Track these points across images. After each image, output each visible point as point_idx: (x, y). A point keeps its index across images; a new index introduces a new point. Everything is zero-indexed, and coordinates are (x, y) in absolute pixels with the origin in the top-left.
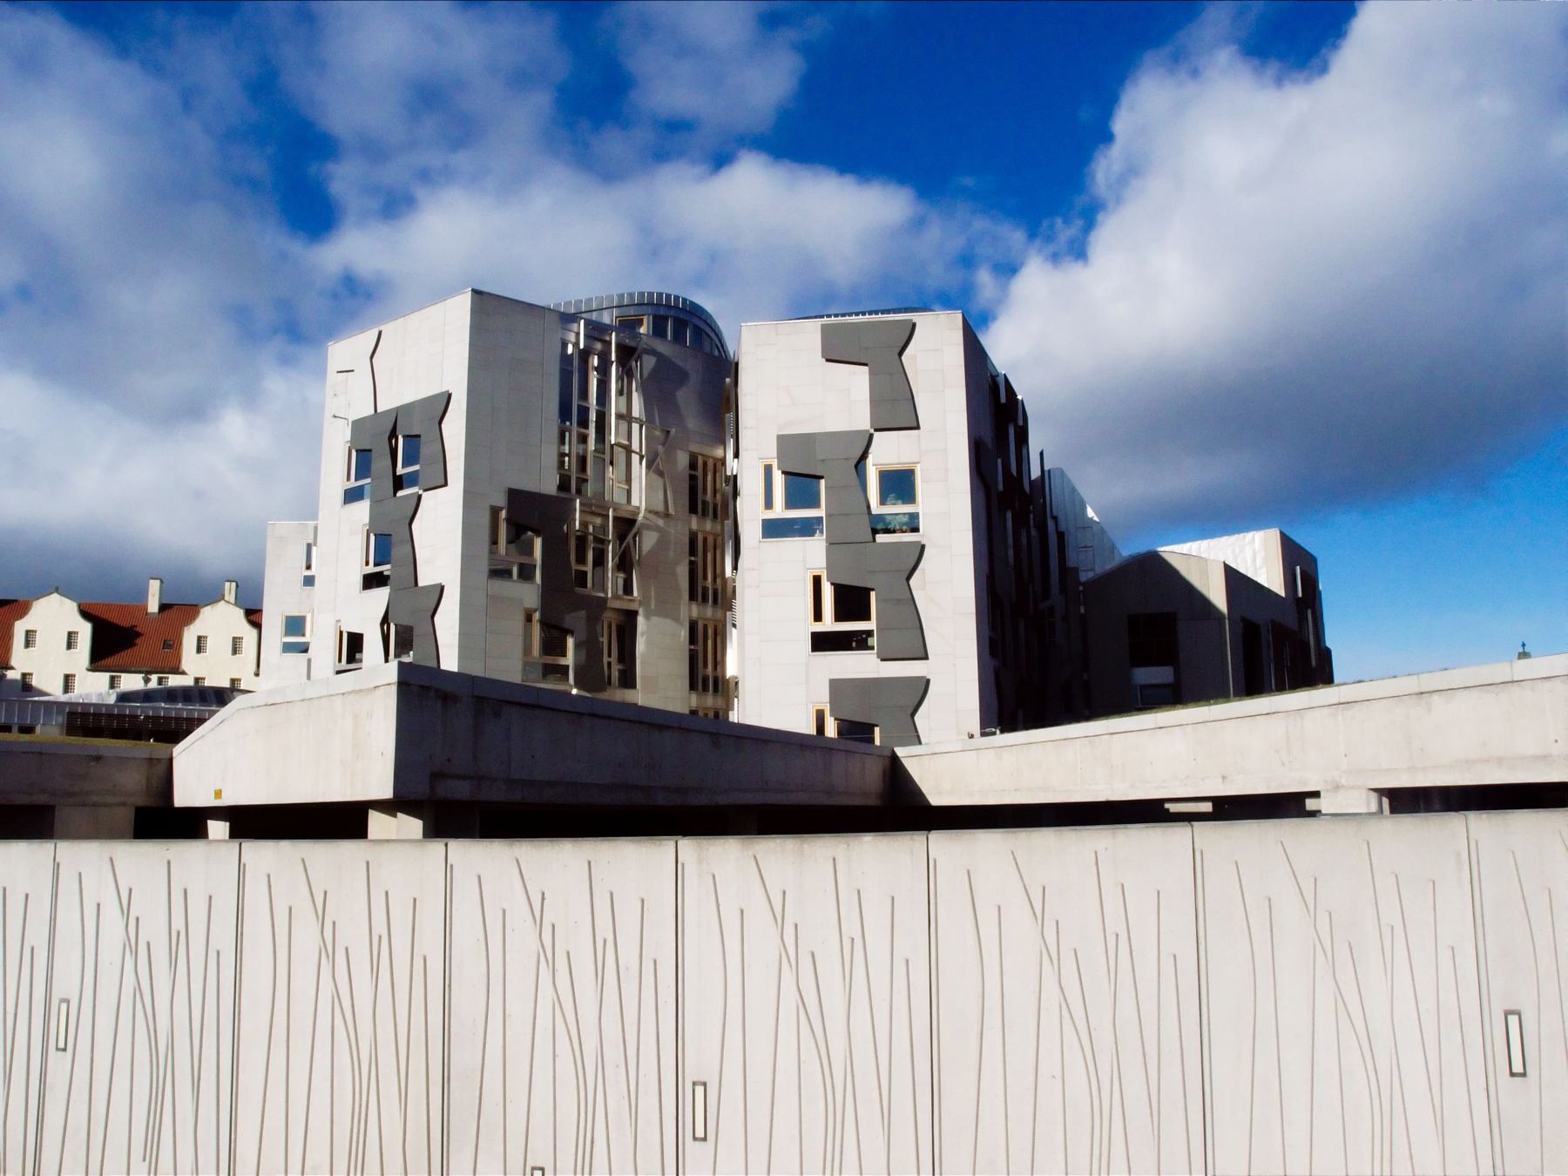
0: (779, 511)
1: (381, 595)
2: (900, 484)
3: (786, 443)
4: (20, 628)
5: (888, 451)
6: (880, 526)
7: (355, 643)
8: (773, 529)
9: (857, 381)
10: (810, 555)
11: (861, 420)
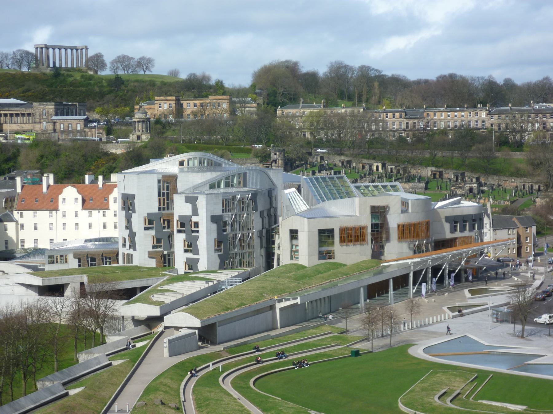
0: (180, 228)
1: (128, 231)
2: (196, 225)
3: (179, 216)
4: (60, 197)
5: (194, 219)
6: (193, 231)
8: (179, 231)
9: (190, 206)
10: (183, 236)
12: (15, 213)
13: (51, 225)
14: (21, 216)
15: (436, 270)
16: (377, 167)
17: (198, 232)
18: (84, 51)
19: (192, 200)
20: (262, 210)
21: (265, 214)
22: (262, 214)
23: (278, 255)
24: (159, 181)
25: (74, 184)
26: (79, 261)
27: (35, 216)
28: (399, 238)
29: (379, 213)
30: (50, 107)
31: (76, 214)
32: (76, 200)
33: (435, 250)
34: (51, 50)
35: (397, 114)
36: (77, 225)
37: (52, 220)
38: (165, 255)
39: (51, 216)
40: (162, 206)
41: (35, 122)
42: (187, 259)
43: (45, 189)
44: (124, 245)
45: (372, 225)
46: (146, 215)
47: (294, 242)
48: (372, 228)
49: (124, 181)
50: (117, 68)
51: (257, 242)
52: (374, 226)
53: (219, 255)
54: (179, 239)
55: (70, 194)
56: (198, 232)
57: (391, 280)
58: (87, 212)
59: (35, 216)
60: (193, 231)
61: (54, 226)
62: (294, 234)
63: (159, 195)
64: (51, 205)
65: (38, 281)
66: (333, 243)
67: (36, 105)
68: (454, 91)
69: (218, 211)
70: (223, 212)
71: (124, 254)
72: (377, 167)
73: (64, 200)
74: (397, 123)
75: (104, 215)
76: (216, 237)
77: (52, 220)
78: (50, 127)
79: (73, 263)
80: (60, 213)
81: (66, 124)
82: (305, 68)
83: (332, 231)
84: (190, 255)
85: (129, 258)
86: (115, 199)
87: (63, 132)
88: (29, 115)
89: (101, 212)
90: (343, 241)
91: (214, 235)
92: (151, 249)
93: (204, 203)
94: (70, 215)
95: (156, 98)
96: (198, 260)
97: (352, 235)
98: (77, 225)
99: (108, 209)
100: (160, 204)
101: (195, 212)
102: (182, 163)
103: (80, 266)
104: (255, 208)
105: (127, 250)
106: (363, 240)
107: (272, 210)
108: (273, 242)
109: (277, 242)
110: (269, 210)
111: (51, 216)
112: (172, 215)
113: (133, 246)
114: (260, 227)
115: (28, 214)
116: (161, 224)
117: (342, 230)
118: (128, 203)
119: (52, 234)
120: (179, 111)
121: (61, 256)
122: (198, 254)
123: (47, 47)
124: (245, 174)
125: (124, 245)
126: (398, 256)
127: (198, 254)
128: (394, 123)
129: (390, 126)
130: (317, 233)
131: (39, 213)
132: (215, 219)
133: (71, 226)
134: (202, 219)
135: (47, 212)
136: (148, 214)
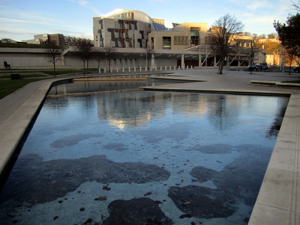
11: (100, 28)
20: (142, 30)
22: (142, 32)
48: (192, 38)
66: (170, 44)
76: (111, 39)
101: (102, 28)
117: (175, 38)
124: (133, 14)
130: (162, 39)
132: (109, 30)
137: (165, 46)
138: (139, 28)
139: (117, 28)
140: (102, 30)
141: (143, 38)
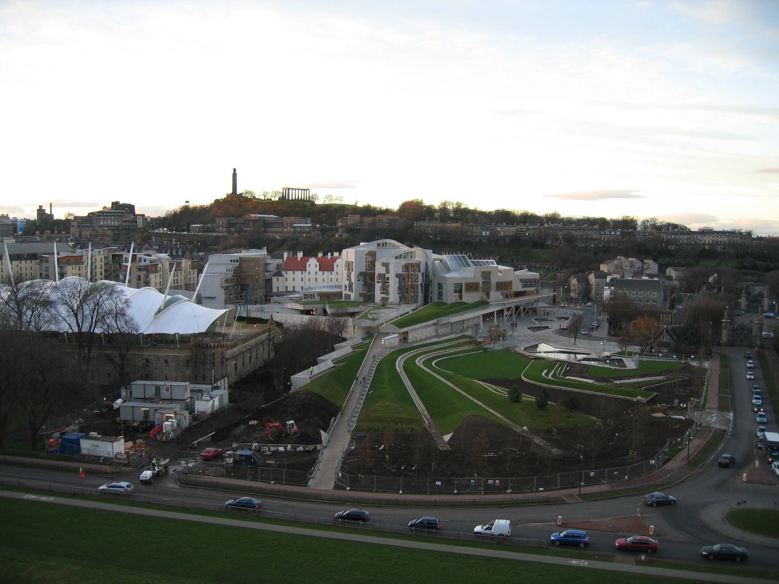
0: (378, 281)
2: (388, 279)
4: (308, 264)
5: (387, 276)
6: (386, 282)
7: (346, 287)
8: (378, 282)
11: (384, 272)
12: (283, 272)
13: (302, 278)
14: (286, 274)
15: (517, 308)
16: (469, 255)
17: (388, 283)
18: (308, 191)
19: (386, 265)
21: (424, 275)
22: (423, 274)
23: (431, 297)
24: (366, 255)
25: (313, 256)
26: (321, 297)
27: (294, 273)
28: (497, 290)
29: (486, 275)
30: (292, 219)
31: (316, 273)
32: (316, 266)
33: (515, 297)
34: (290, 190)
35: (479, 228)
36: (316, 279)
37: (303, 276)
38: (369, 296)
39: (302, 274)
40: (368, 268)
41: (283, 227)
42: (382, 297)
43: (299, 259)
44: (346, 290)
45: (483, 282)
46: (359, 273)
47: (441, 290)
49: (349, 254)
50: (325, 201)
51: (420, 289)
52: (485, 283)
53: (399, 296)
54: (378, 286)
55: (313, 263)
56: (388, 283)
57: (496, 313)
58: (321, 272)
59: (294, 273)
60: (386, 282)
61: (304, 279)
62: (440, 286)
63: (366, 262)
64: (303, 268)
65: (300, 307)
67: (285, 218)
68: (504, 217)
69: (400, 271)
70: (403, 271)
71: (345, 294)
72: (469, 255)
73: (309, 265)
74: (478, 232)
75: (331, 274)
76: (398, 286)
77: (303, 276)
78: (292, 230)
79: (317, 298)
80: (307, 272)
81: (301, 228)
82: (427, 203)
83: (462, 284)
84: (384, 295)
85: (348, 296)
86: (337, 265)
87: (299, 232)
88: (281, 223)
89: (330, 272)
90: (467, 290)
91: (397, 285)
92: (361, 292)
93: (393, 266)
94: (313, 273)
95: (349, 216)
96: (388, 298)
97: (472, 287)
98: (316, 279)
99: (333, 271)
100: (366, 267)
101: (388, 271)
102: (379, 245)
103: (321, 300)
104: (419, 271)
105: (347, 292)
106: (477, 290)
107: (427, 272)
108: (429, 291)
109: (430, 290)
110: (426, 273)
111: (302, 274)
112: (374, 274)
113: (351, 289)
114: (421, 282)
115: (290, 273)
116: (368, 278)
118: (349, 265)
119: (302, 284)
120: (362, 222)
121: (311, 295)
122: (389, 295)
123: (289, 189)
125: (346, 290)
126: (497, 301)
127: (389, 295)
128: (477, 232)
129: (475, 234)
130: (453, 285)
131: (295, 272)
132: (397, 276)
133: (313, 280)
134: (392, 276)
135: (300, 272)
136: (360, 273)
137: (455, 294)
138: (422, 271)
139: (403, 273)
140: (387, 276)
141: (423, 282)
